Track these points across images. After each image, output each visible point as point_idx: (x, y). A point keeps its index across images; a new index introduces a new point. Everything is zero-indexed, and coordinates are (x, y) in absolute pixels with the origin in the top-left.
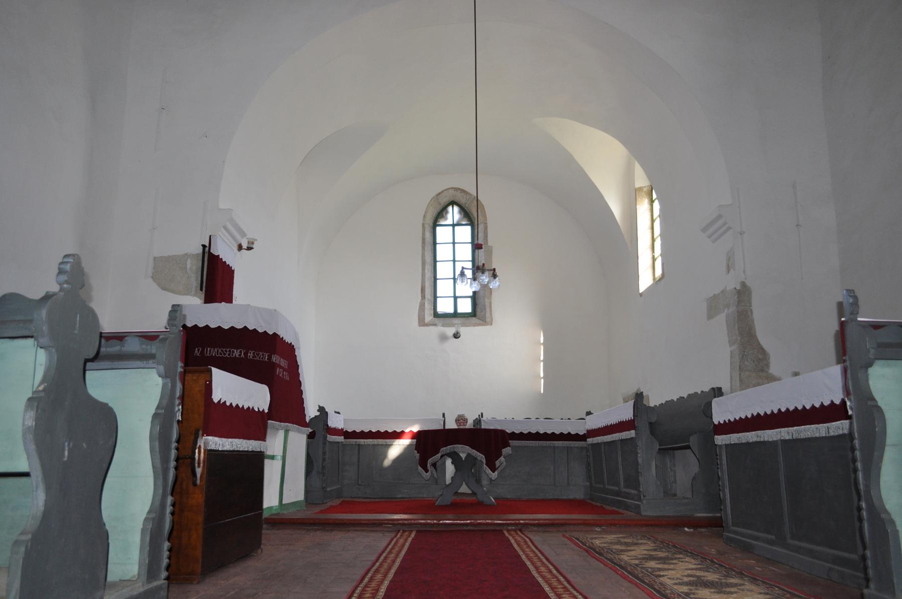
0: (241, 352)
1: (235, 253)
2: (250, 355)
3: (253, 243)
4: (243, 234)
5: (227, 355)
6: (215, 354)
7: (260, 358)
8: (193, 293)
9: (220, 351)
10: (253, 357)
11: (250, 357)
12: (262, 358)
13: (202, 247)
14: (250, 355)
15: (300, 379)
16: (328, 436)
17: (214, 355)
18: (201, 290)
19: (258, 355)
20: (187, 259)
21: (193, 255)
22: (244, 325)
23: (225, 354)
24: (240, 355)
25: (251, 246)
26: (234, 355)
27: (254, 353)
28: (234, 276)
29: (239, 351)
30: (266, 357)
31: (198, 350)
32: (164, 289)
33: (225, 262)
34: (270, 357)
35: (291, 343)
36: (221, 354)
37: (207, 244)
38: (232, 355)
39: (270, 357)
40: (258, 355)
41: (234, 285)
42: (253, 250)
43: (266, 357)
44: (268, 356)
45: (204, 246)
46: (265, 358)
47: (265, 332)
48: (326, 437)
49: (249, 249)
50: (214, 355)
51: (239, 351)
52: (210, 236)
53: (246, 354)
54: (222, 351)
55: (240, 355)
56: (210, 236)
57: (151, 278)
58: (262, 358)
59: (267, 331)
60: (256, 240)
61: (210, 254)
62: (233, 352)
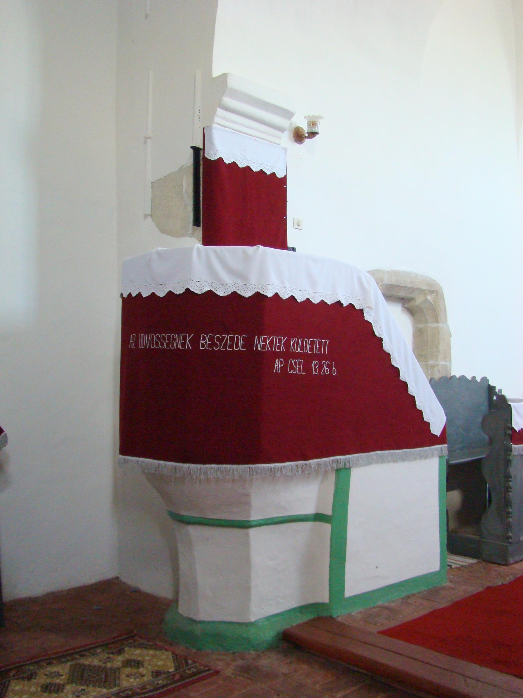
0: (184, 338)
1: (285, 149)
2: (205, 342)
3: (314, 124)
4: (288, 114)
5: (165, 346)
6: (150, 346)
7: (225, 346)
8: (191, 231)
9: (155, 339)
10: (210, 346)
11: (203, 345)
12: (231, 346)
13: (191, 151)
14: (205, 342)
15: (394, 363)
16: (513, 446)
17: (148, 347)
18: (196, 223)
19: (220, 340)
20: (183, 176)
21: (188, 167)
22: (186, 288)
23: (162, 344)
24: (184, 344)
25: (314, 130)
26: (175, 345)
27: (211, 339)
28: (285, 189)
29: (181, 336)
30: (241, 343)
31: (133, 336)
32: (163, 231)
33: (248, 169)
34: (249, 343)
35: (339, 303)
36: (157, 344)
37: (201, 147)
38: (173, 344)
39: (249, 343)
40: (220, 340)
41: (288, 203)
42: (317, 136)
43: (241, 343)
44: (244, 339)
45: (197, 151)
46: (237, 346)
47: (235, 293)
48: (510, 449)
49: (312, 134)
50: (148, 347)
51: (181, 336)
52: (204, 129)
53: (195, 342)
54: (158, 338)
55: (184, 344)
56: (204, 129)
57: (149, 218)
58: (231, 346)
59: (239, 292)
60: (322, 118)
61: (205, 159)
62: (174, 339)
